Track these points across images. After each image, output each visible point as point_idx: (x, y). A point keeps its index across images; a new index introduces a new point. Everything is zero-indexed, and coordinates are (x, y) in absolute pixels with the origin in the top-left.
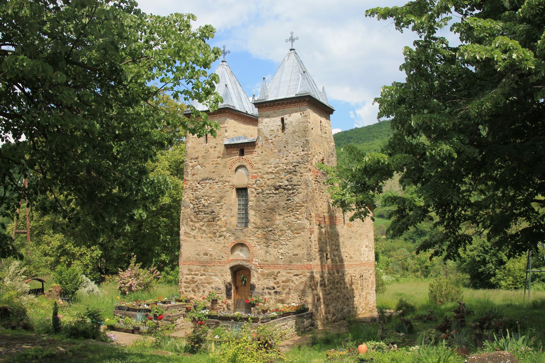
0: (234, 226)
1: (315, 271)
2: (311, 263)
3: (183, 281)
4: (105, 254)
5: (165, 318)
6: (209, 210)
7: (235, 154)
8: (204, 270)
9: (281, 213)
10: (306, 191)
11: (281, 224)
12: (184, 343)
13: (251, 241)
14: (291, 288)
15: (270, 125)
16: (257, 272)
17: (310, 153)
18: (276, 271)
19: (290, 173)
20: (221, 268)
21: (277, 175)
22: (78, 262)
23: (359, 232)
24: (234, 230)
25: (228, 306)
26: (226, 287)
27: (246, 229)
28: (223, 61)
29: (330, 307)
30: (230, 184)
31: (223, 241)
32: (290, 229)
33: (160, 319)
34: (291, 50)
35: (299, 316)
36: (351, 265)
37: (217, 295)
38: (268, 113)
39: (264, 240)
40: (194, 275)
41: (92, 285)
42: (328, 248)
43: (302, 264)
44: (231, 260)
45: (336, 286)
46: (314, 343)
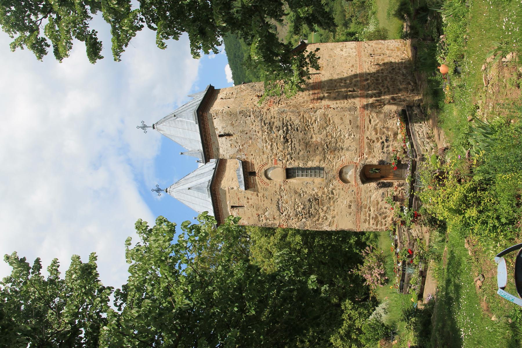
0: (323, 181)
1: (365, 103)
2: (358, 107)
3: (375, 228)
4: (349, 296)
5: (411, 247)
6: (307, 204)
7: (255, 180)
9: (310, 137)
10: (289, 113)
11: (321, 136)
12: (436, 233)
13: (337, 164)
14: (382, 127)
15: (226, 147)
16: (367, 159)
17: (252, 110)
18: (366, 141)
19: (271, 128)
21: (273, 140)
22: (357, 321)
23: (328, 58)
24: (327, 181)
25: (399, 185)
26: (381, 187)
27: (325, 169)
28: (167, 192)
29: (401, 87)
30: (282, 184)
32: (325, 128)
33: (412, 252)
34: (154, 128)
35: (410, 119)
36: (360, 66)
37: (389, 196)
38: (214, 149)
39: (336, 152)
40: (369, 217)
41: (379, 309)
42: (343, 90)
43: (359, 116)
44: (355, 183)
45: (380, 81)
46: (437, 108)
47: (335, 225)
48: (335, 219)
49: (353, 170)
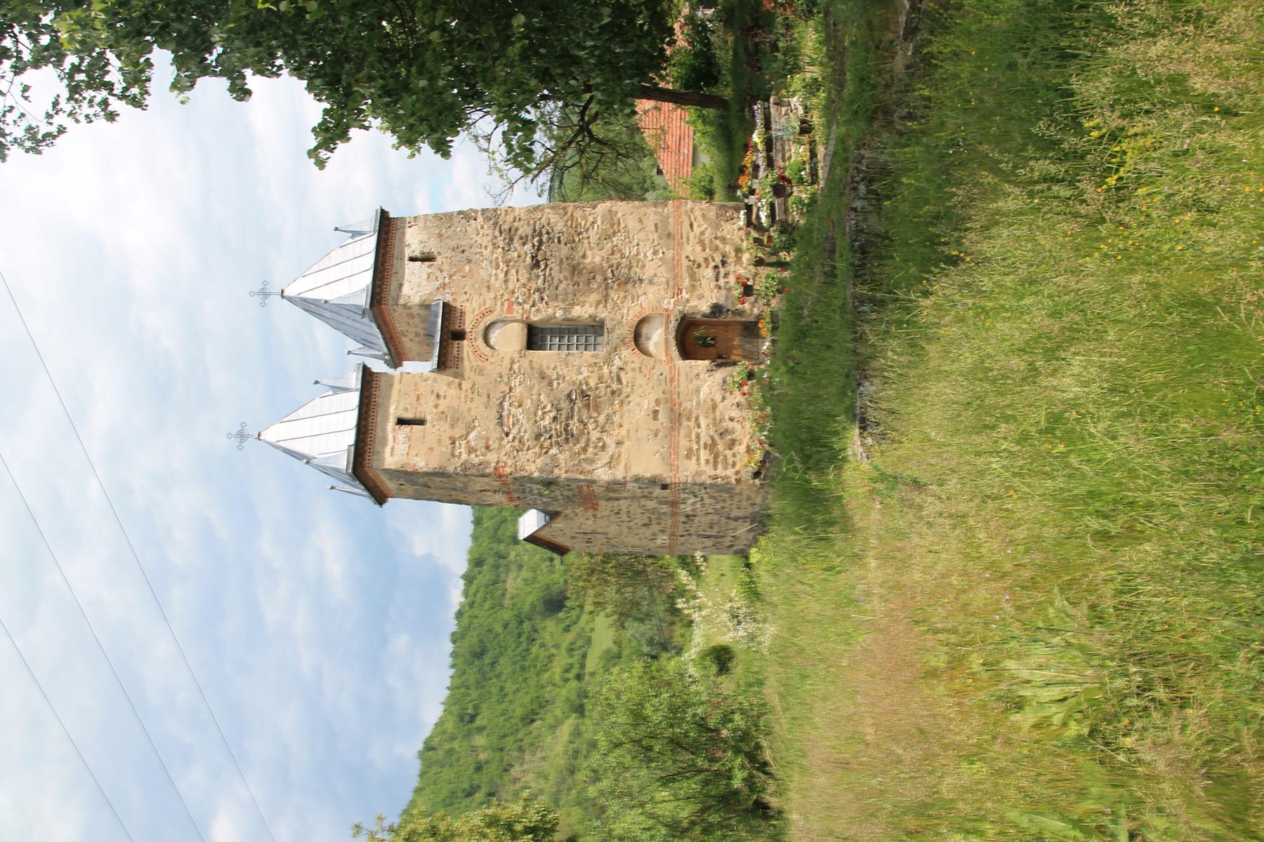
3: (711, 472)
8: (689, 420)
9: (581, 254)
11: (603, 253)
13: (630, 312)
15: (417, 280)
16: (688, 301)
18: (685, 263)
19: (511, 240)
30: (516, 356)
31: (631, 374)
38: (393, 286)
39: (629, 286)
40: (698, 443)
48: (623, 449)
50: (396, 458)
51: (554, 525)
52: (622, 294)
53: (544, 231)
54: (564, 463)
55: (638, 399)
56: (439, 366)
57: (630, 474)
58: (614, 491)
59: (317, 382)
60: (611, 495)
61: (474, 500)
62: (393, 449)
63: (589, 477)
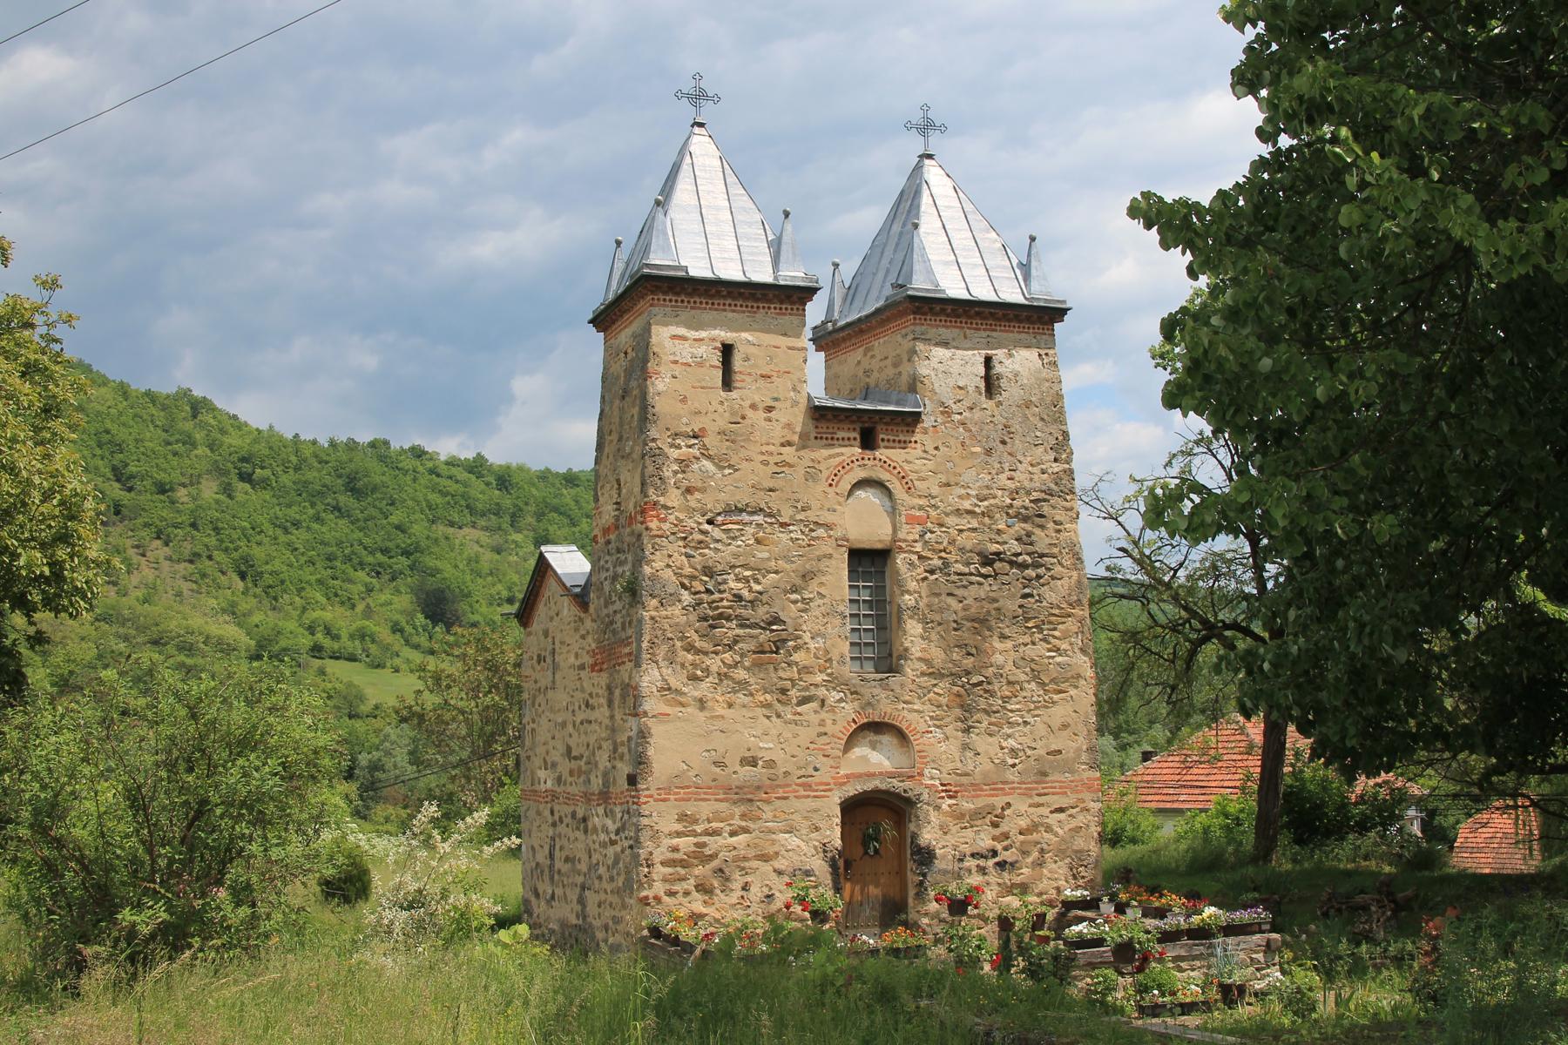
3: (658, 857)
8: (743, 816)
9: (1007, 631)
11: (1010, 666)
13: (914, 716)
15: (955, 369)
16: (938, 808)
18: (999, 801)
19: (1025, 519)
20: (810, 804)
24: (856, 681)
30: (838, 533)
38: (945, 333)
39: (958, 712)
40: (707, 833)
44: (847, 776)
47: (668, 710)
49: (887, 765)
50: (668, 343)
51: (566, 601)
52: (944, 700)
53: (1041, 571)
54: (666, 614)
55: (774, 732)
56: (817, 408)
57: (650, 722)
58: (624, 697)
59: (787, 214)
60: (617, 692)
61: (603, 471)
62: (684, 338)
63: (645, 656)
